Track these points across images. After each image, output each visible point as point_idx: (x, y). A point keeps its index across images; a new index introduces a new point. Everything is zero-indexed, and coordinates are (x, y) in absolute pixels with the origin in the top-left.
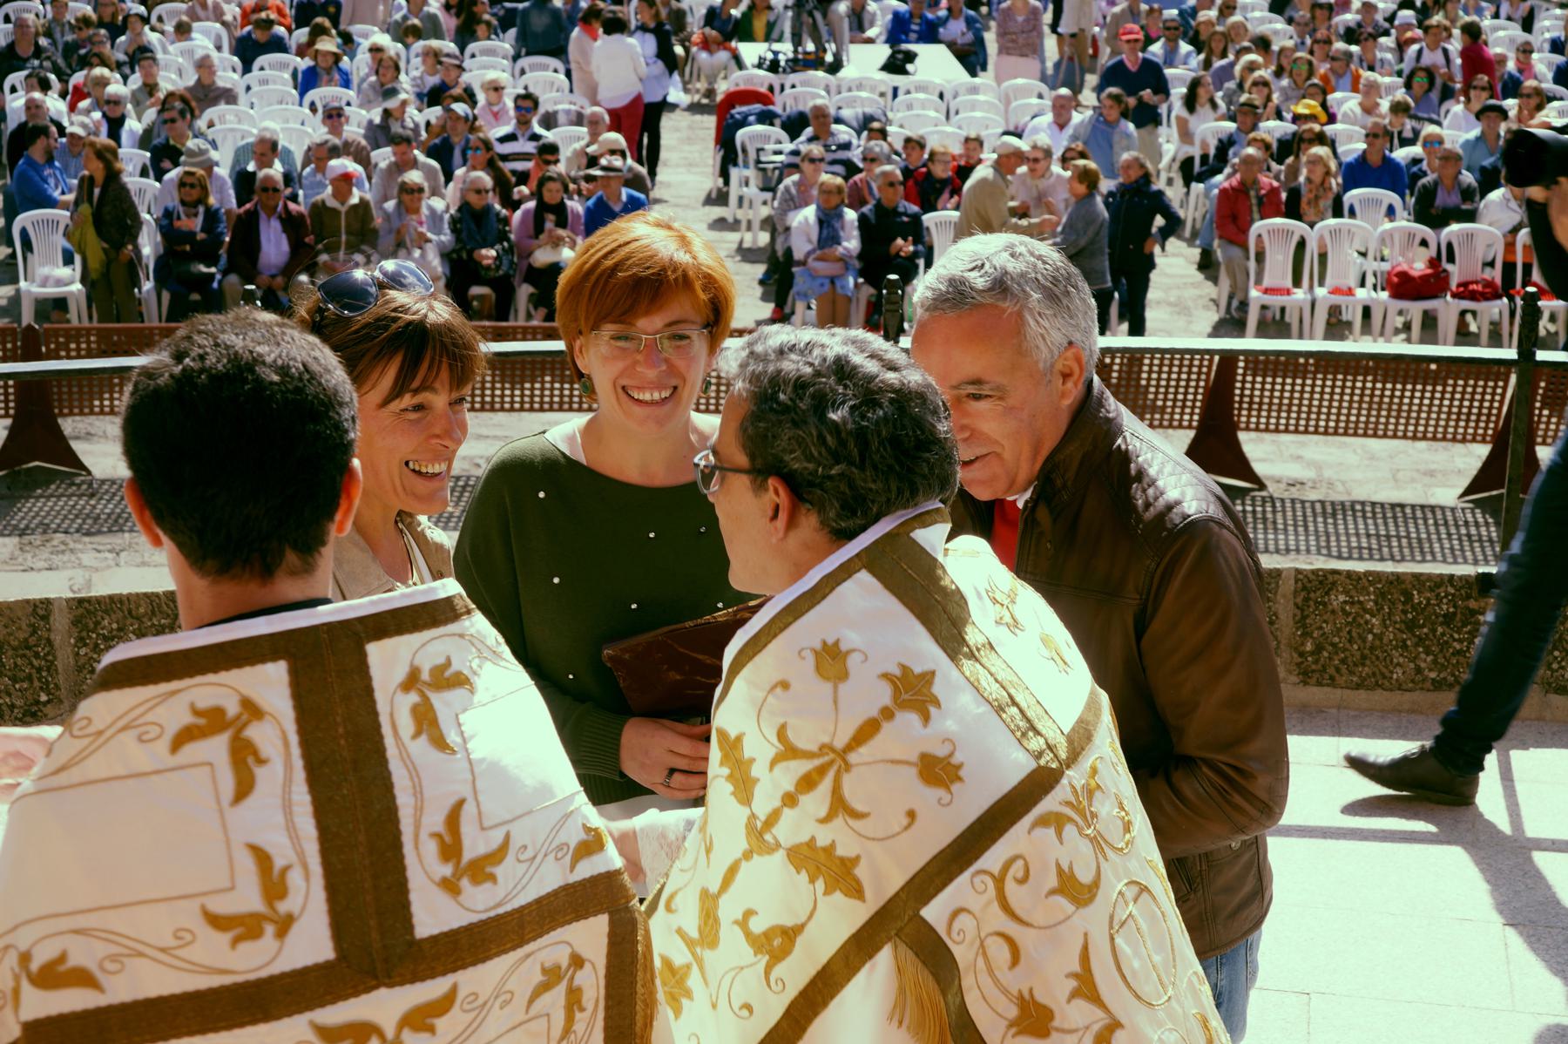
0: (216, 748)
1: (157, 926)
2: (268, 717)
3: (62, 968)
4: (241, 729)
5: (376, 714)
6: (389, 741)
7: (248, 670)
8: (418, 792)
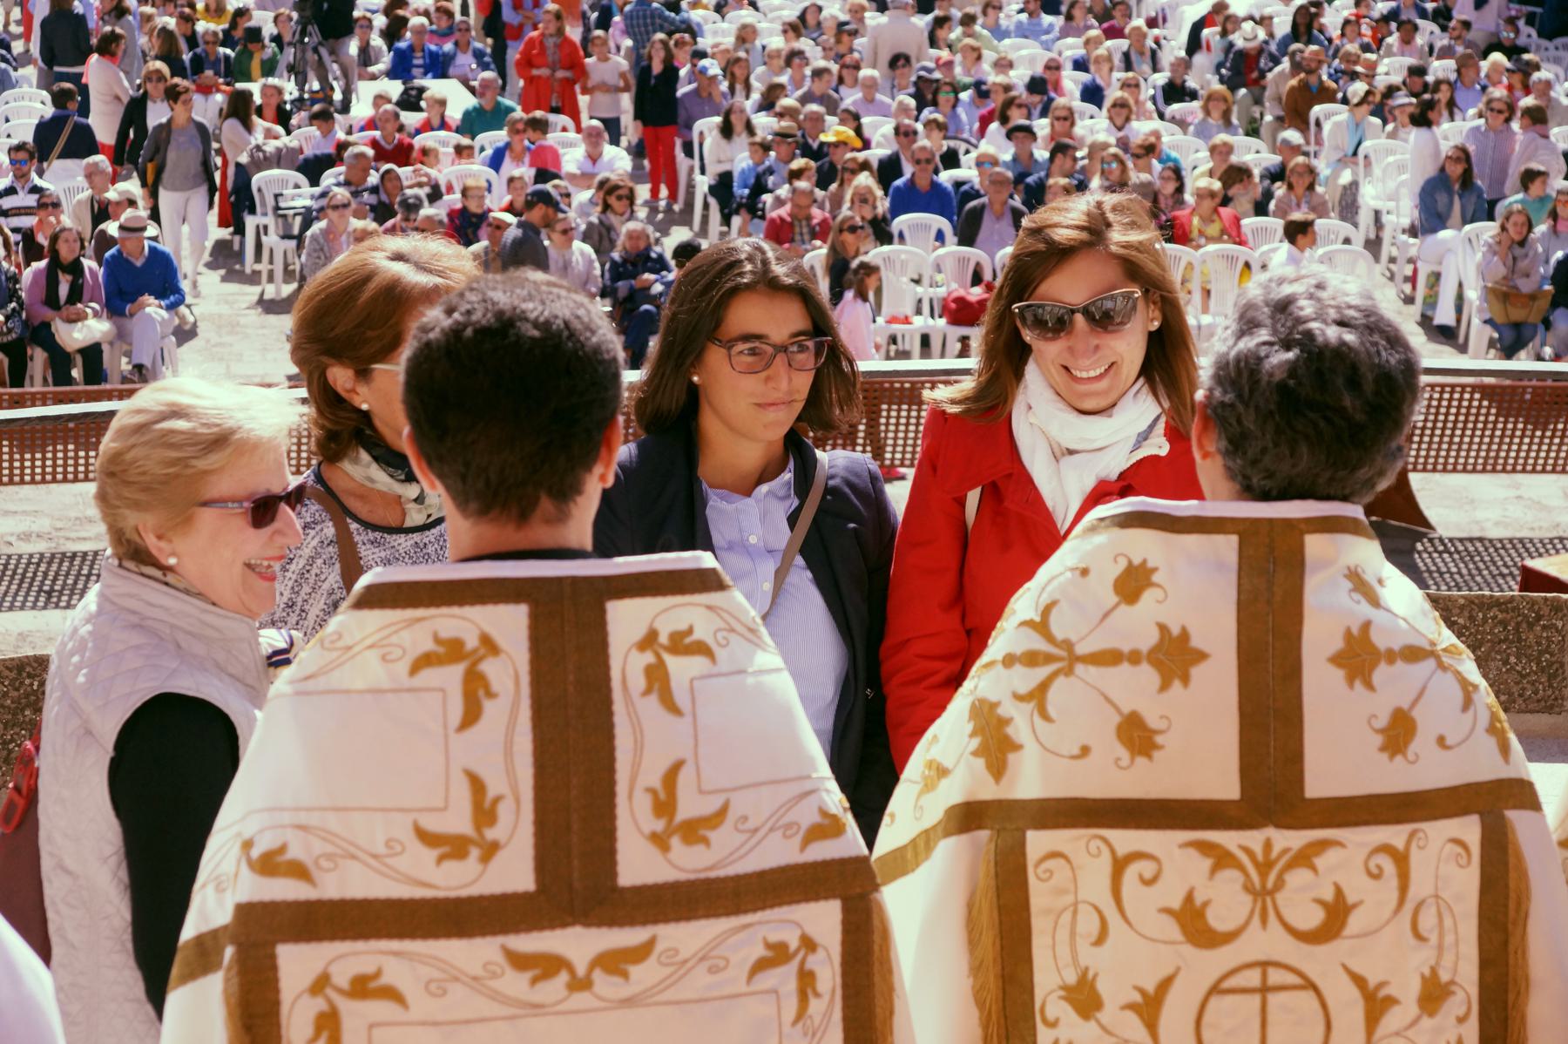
0: (452, 675)
1: (373, 833)
2: (503, 656)
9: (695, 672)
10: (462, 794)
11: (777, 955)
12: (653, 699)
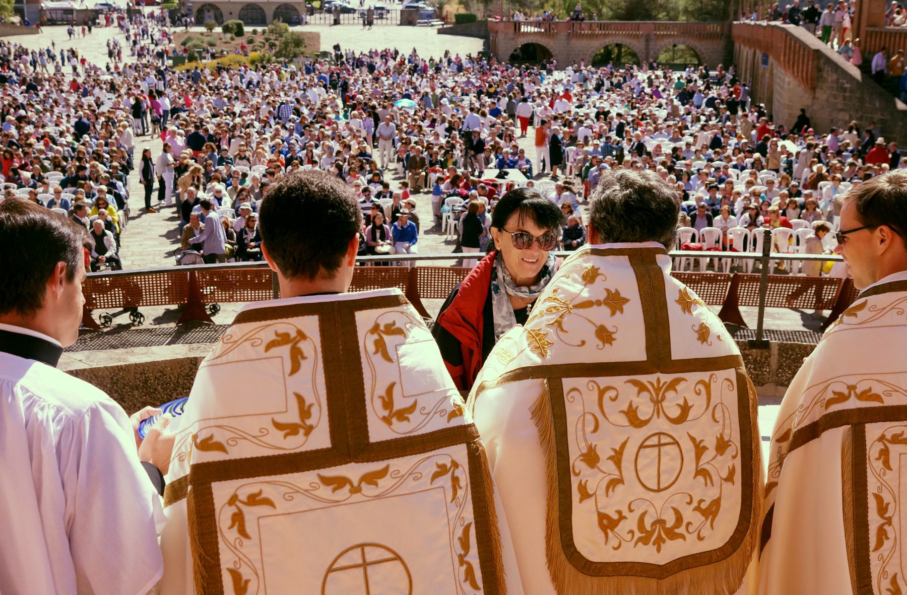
0: (285, 351)
1: (252, 426)
3: (210, 442)
4: (296, 343)
5: (357, 342)
6: (363, 354)
7: (301, 318)
8: (374, 378)
9: (397, 343)
10: (294, 404)
11: (442, 470)
12: (379, 355)
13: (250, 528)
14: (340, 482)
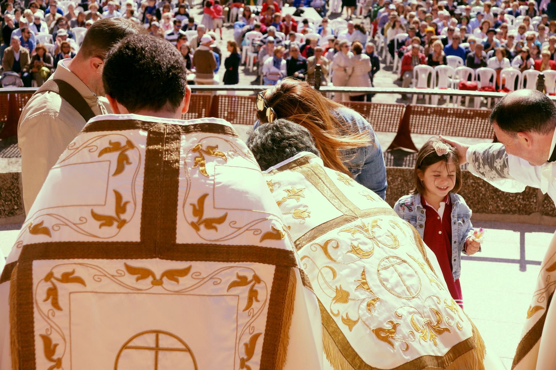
8: (189, 186)
13: (62, 301)
14: (144, 274)
